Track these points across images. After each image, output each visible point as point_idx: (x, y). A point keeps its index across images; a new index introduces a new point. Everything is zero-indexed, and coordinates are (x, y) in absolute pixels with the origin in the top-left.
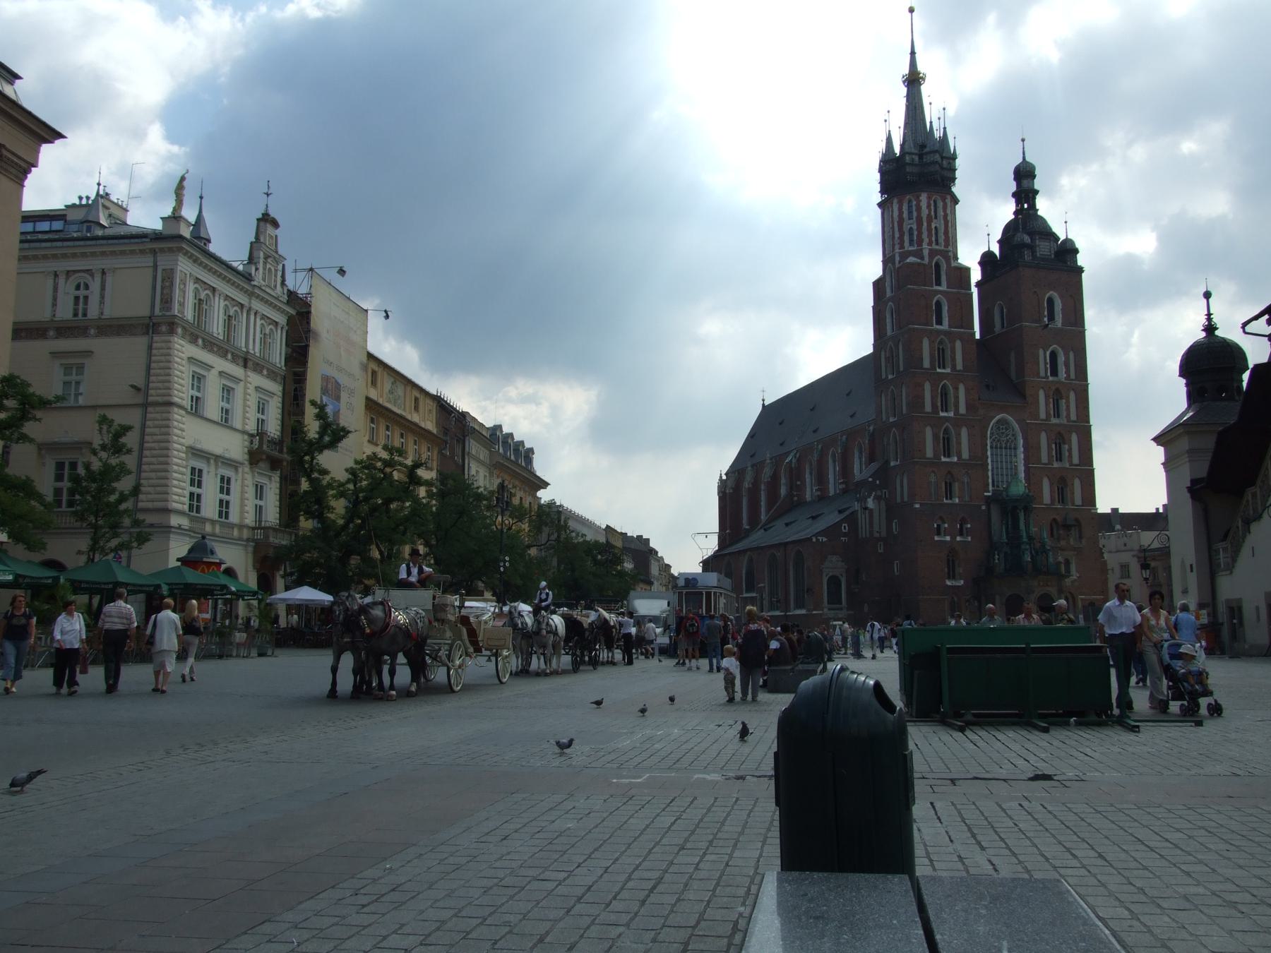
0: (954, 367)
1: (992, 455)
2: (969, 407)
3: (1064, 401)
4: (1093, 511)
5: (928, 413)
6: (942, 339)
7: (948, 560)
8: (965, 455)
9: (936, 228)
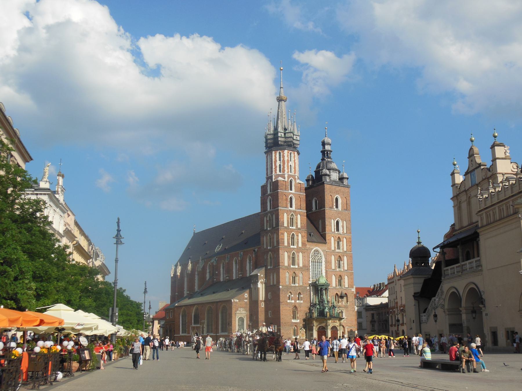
0: (297, 226)
2: (303, 244)
3: (341, 242)
6: (292, 214)
7: (293, 311)
8: (301, 265)
9: (291, 165)
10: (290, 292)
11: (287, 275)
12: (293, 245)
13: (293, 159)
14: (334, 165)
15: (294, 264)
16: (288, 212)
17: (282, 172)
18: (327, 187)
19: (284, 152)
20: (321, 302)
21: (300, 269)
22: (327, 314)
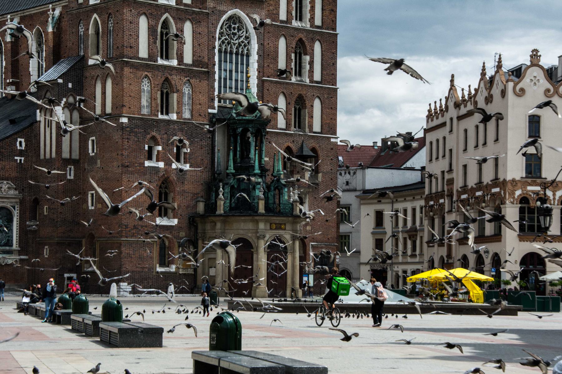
1: (220, 61)
4: (332, 140)
8: (188, 59)
11: (146, 86)
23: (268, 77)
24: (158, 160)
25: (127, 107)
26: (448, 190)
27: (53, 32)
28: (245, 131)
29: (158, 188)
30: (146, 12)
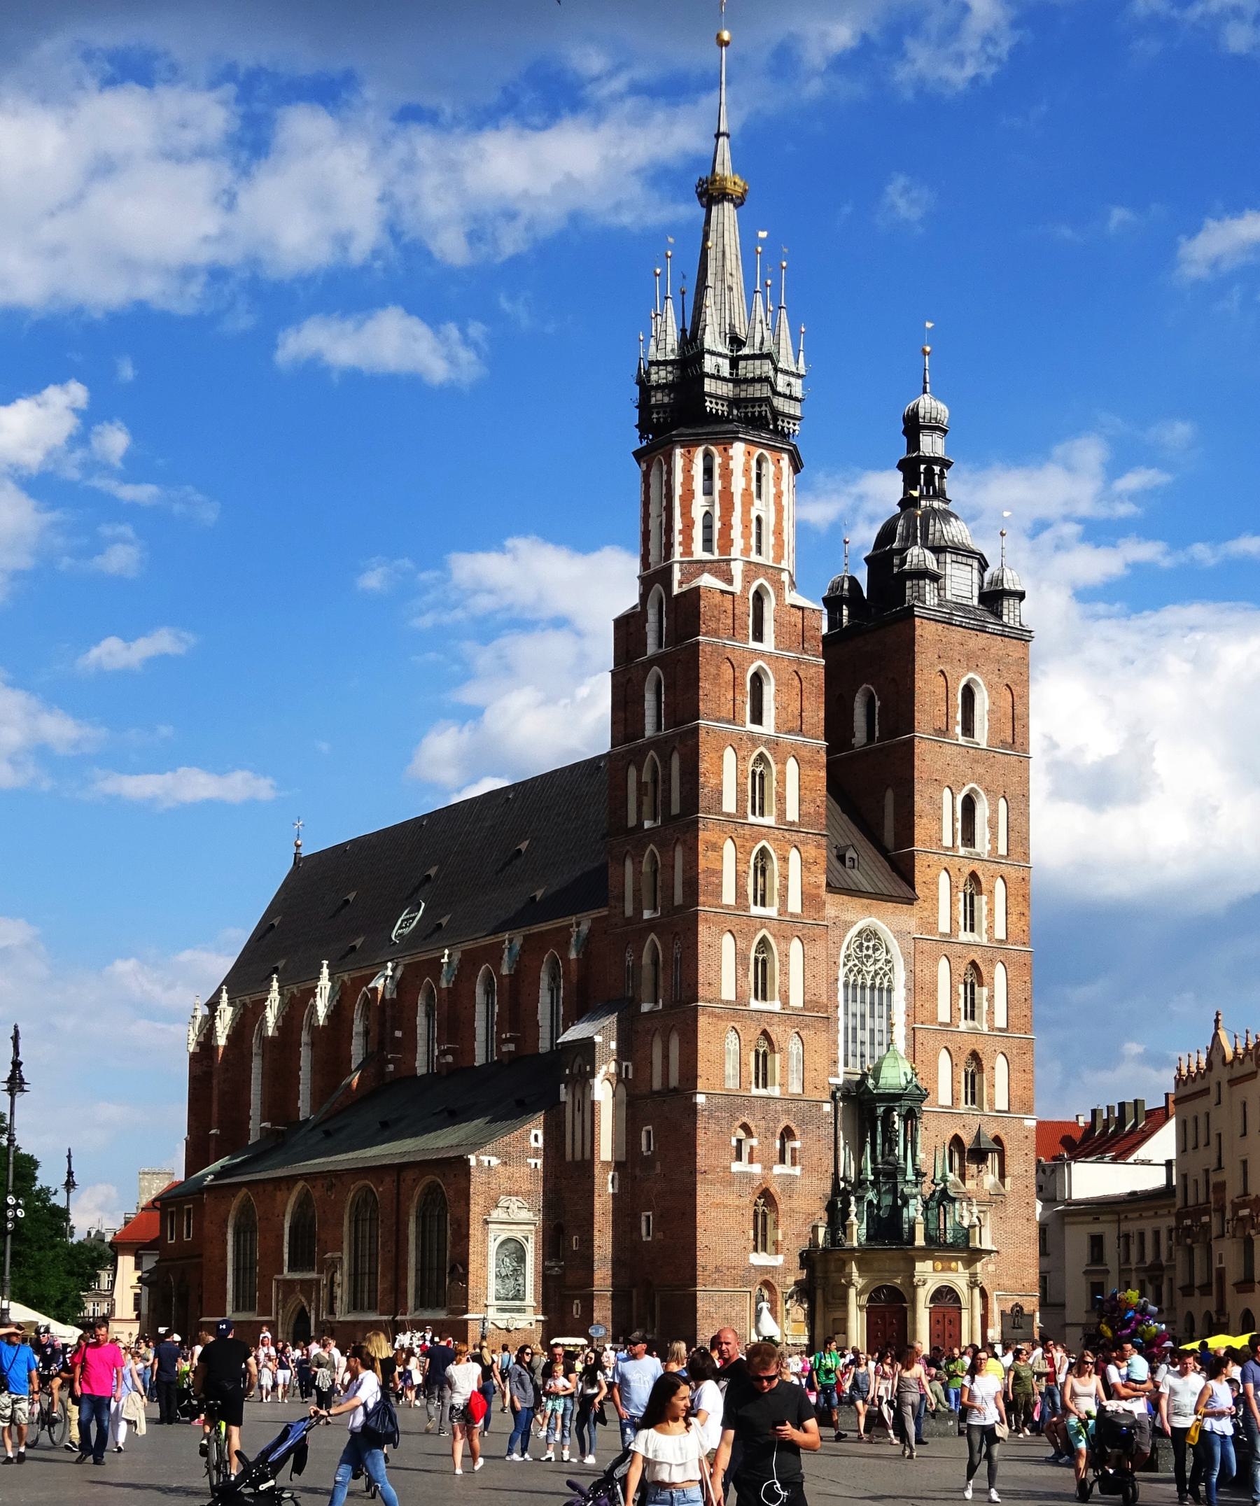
0: (782, 813)
1: (846, 1001)
2: (808, 898)
3: (984, 898)
5: (728, 907)
6: (761, 755)
7: (756, 1214)
8: (796, 1000)
9: (759, 519)
10: (745, 1127)
11: (732, 1042)
12: (763, 904)
13: (773, 490)
14: (956, 531)
15: (762, 992)
16: (742, 743)
17: (716, 551)
18: (925, 631)
19: (731, 452)
20: (889, 1174)
21: (788, 1016)
22: (912, 1229)
23: (922, 1023)
24: (751, 1161)
25: (704, 1078)
26: (1216, 1201)
27: (578, 960)
28: (889, 1111)
29: (752, 1205)
30: (732, 928)
